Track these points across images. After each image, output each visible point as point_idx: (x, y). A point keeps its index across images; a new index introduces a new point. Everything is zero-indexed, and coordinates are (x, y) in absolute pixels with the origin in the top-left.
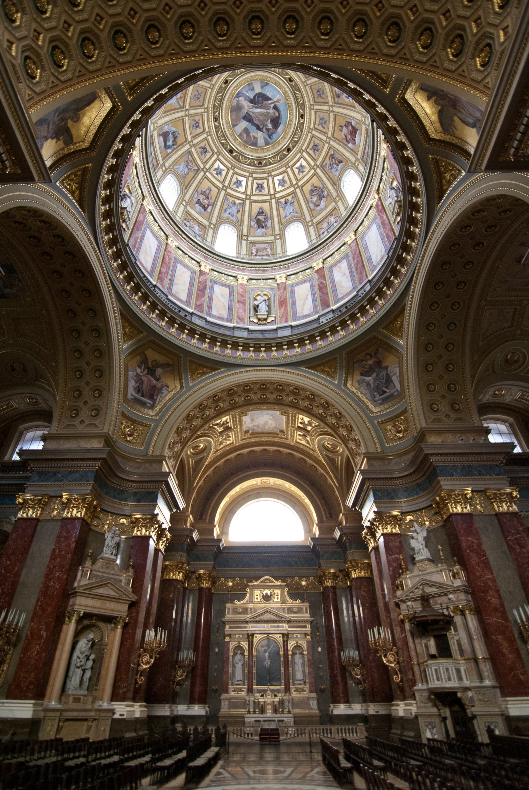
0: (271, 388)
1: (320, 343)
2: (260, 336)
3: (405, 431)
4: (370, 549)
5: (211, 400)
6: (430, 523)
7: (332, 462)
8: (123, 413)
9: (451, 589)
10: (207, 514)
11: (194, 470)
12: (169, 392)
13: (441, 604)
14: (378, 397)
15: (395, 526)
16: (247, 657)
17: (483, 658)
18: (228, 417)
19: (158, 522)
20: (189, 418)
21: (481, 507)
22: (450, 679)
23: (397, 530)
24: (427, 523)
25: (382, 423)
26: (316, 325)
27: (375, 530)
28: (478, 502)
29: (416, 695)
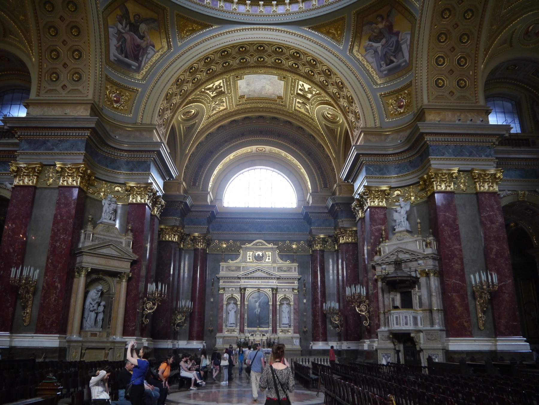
0: (270, 50)
3: (408, 106)
4: (357, 219)
5: (203, 63)
6: (415, 198)
7: (331, 132)
8: (107, 76)
9: (421, 256)
10: (200, 180)
11: (185, 136)
12: (155, 52)
13: (410, 268)
14: (384, 67)
15: (382, 199)
17: (438, 310)
18: (221, 81)
19: (152, 190)
20: (179, 83)
21: (465, 185)
22: (406, 324)
23: (384, 204)
24: (413, 198)
25: (385, 95)
27: (364, 203)
28: (462, 181)
29: (379, 335)
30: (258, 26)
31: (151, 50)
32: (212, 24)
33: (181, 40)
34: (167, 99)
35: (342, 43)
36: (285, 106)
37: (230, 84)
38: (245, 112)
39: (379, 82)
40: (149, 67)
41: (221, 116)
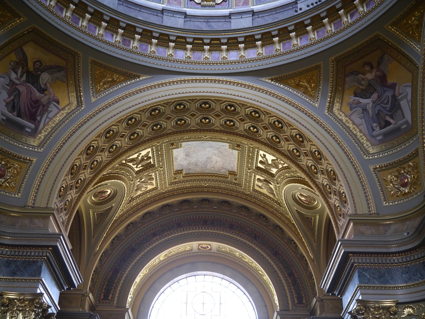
0: (218, 108)
1: (296, 42)
2: (204, 26)
3: (415, 183)
5: (124, 125)
10: (115, 292)
11: (97, 225)
12: (60, 110)
14: (378, 131)
18: (150, 150)
19: (42, 304)
25: (381, 169)
26: (291, 13)
30: (202, 77)
31: (54, 108)
32: (138, 74)
33: (96, 94)
34: (72, 174)
36: (239, 185)
37: (162, 155)
38: (183, 194)
39: (371, 151)
40: (50, 130)
41: (148, 199)
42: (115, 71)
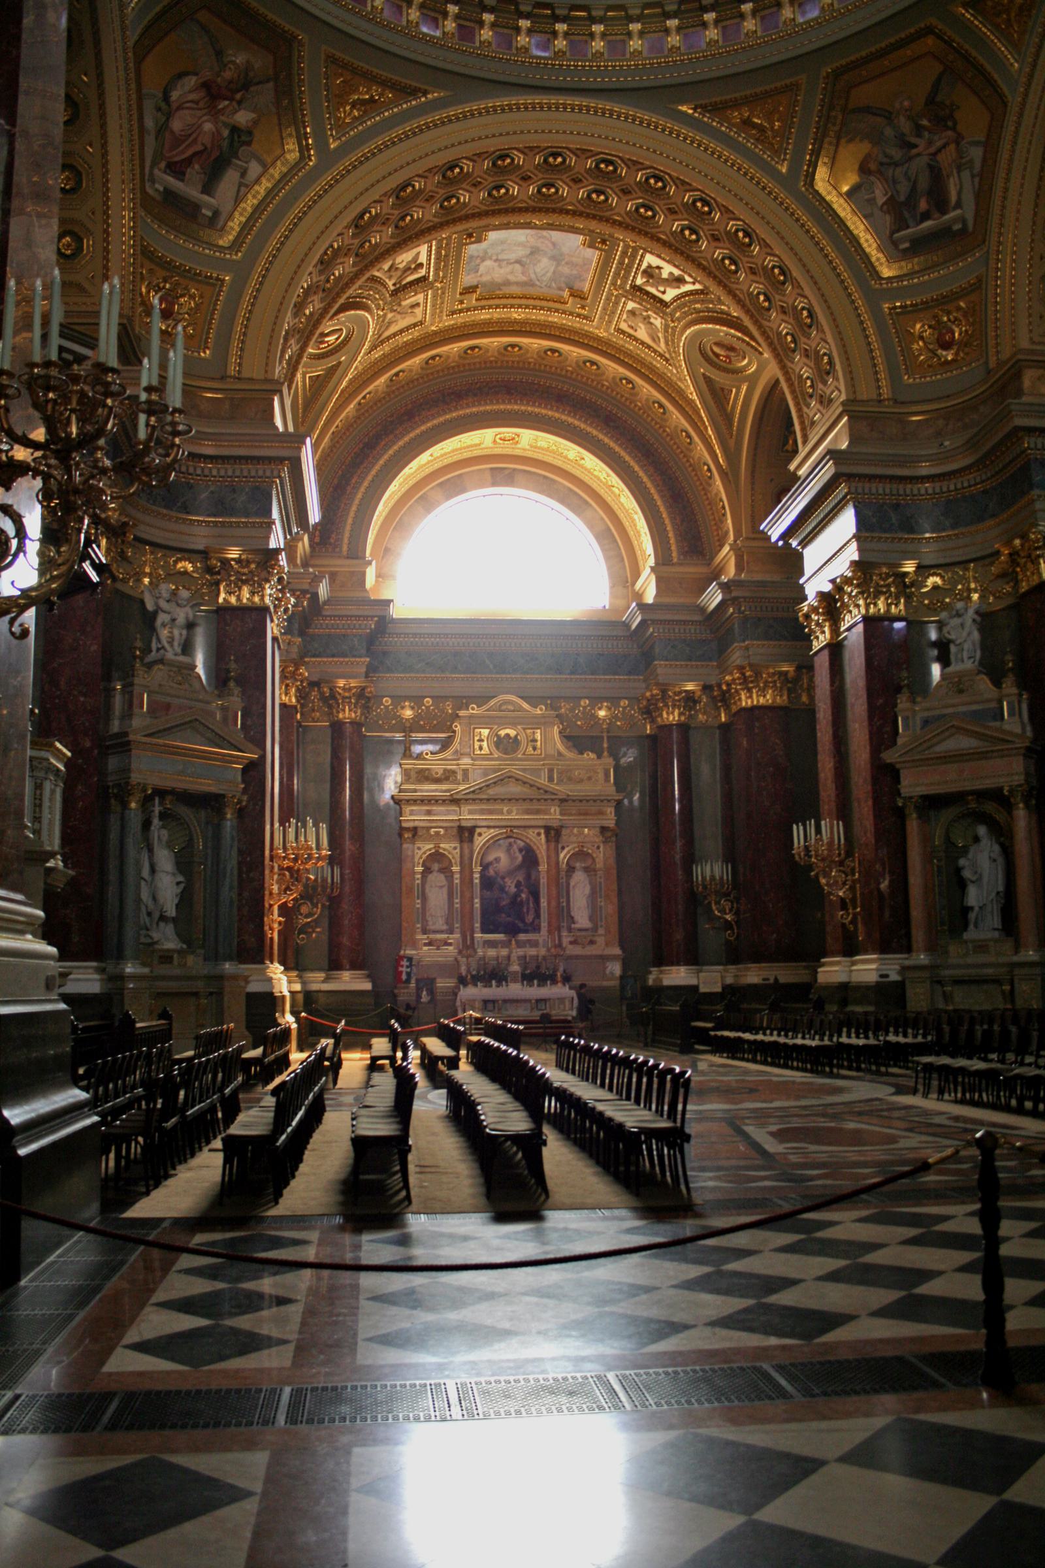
3: (964, 344)
7: (717, 396)
15: (897, 598)
16: (457, 876)
35: (786, 154)
39: (886, 272)
41: (406, 344)
42: (371, 79)
